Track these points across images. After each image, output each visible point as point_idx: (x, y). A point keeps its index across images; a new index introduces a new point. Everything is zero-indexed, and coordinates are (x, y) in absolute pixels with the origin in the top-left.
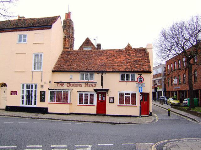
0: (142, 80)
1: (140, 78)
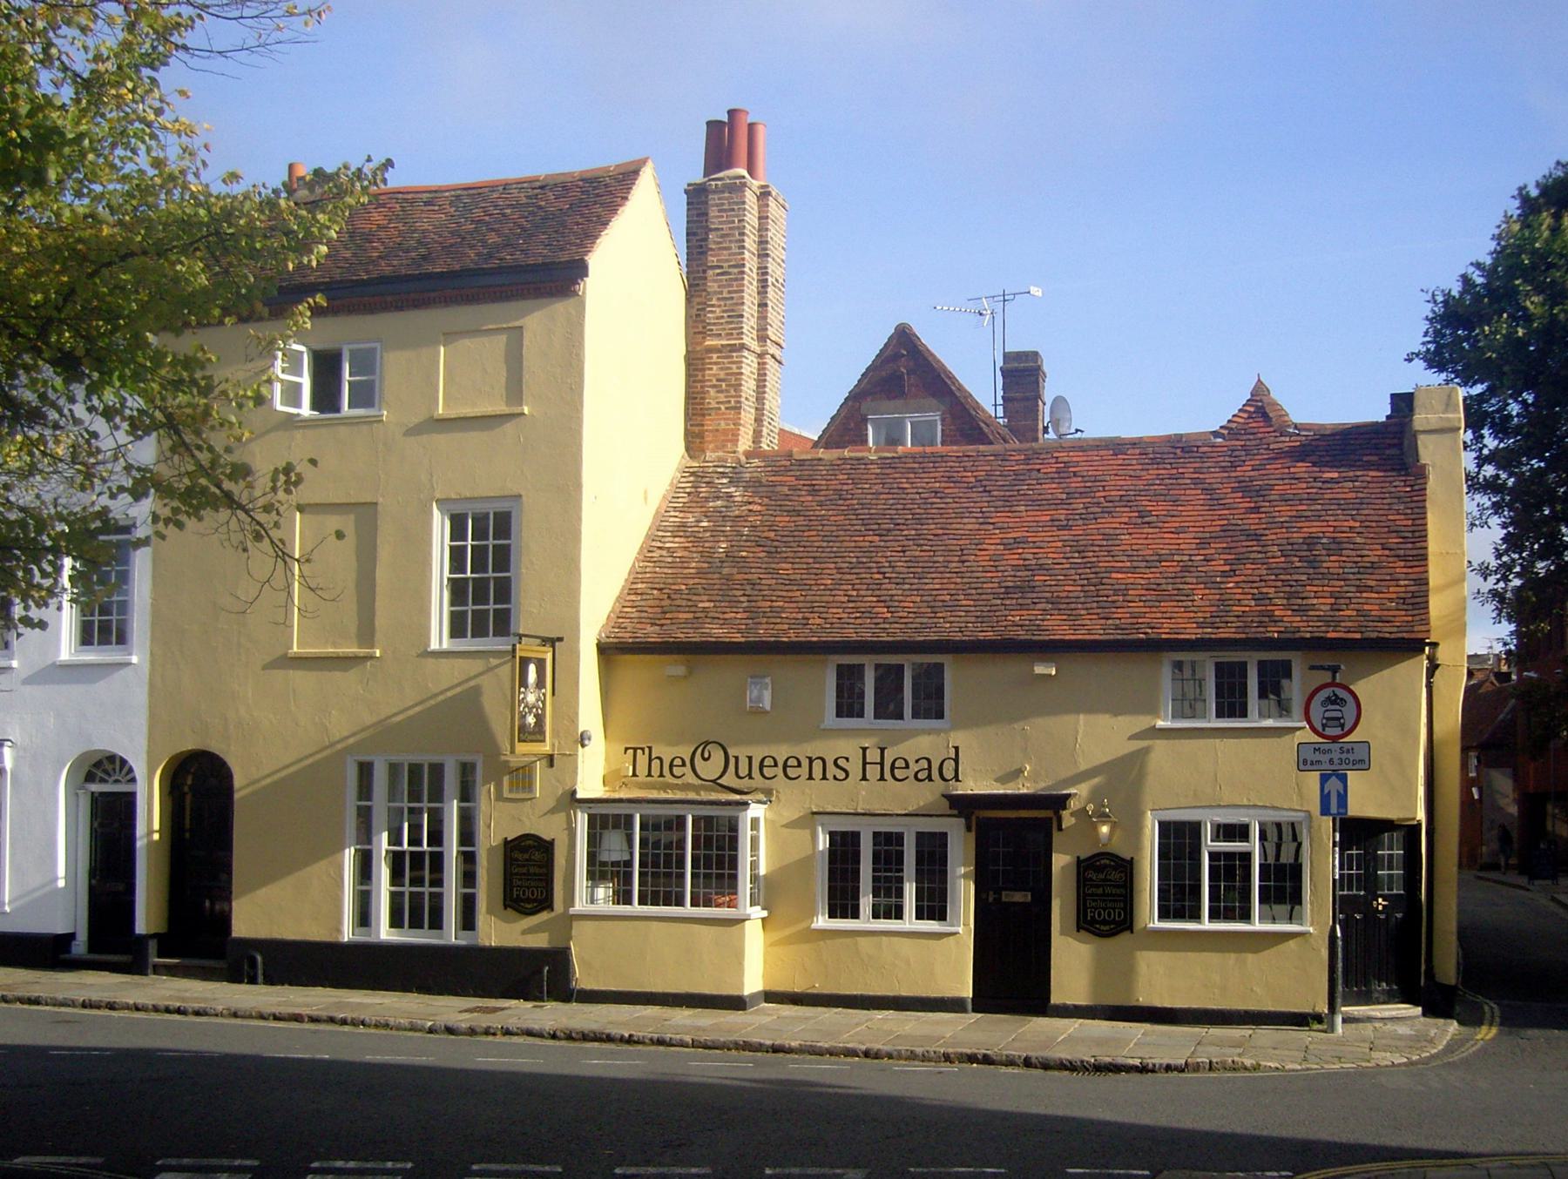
0: (1349, 712)
1: (1335, 700)
